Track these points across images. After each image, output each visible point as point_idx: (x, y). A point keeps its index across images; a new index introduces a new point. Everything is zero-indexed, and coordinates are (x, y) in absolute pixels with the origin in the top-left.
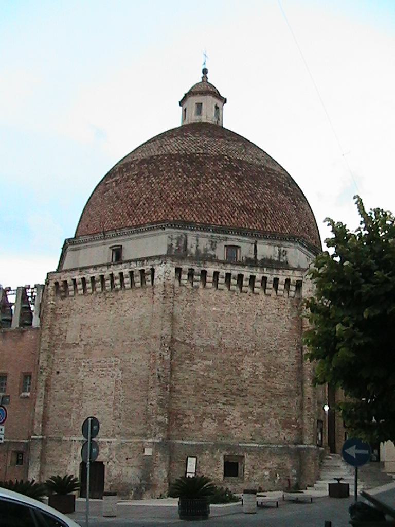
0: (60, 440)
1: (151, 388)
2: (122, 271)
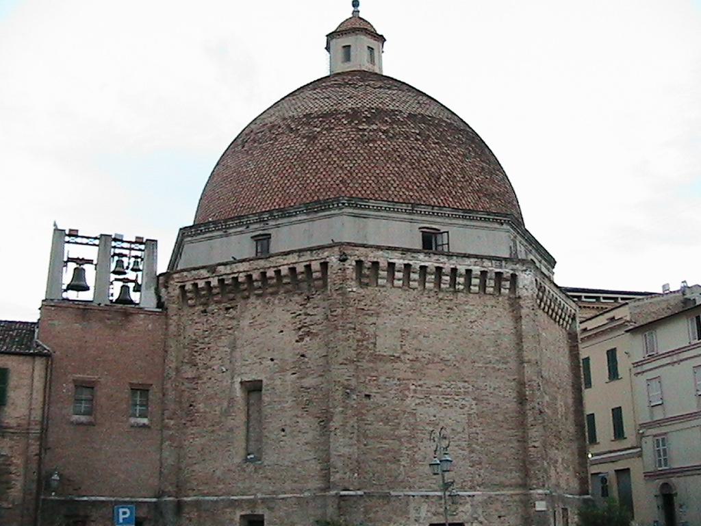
0: (387, 497)
1: (532, 425)
2: (470, 268)
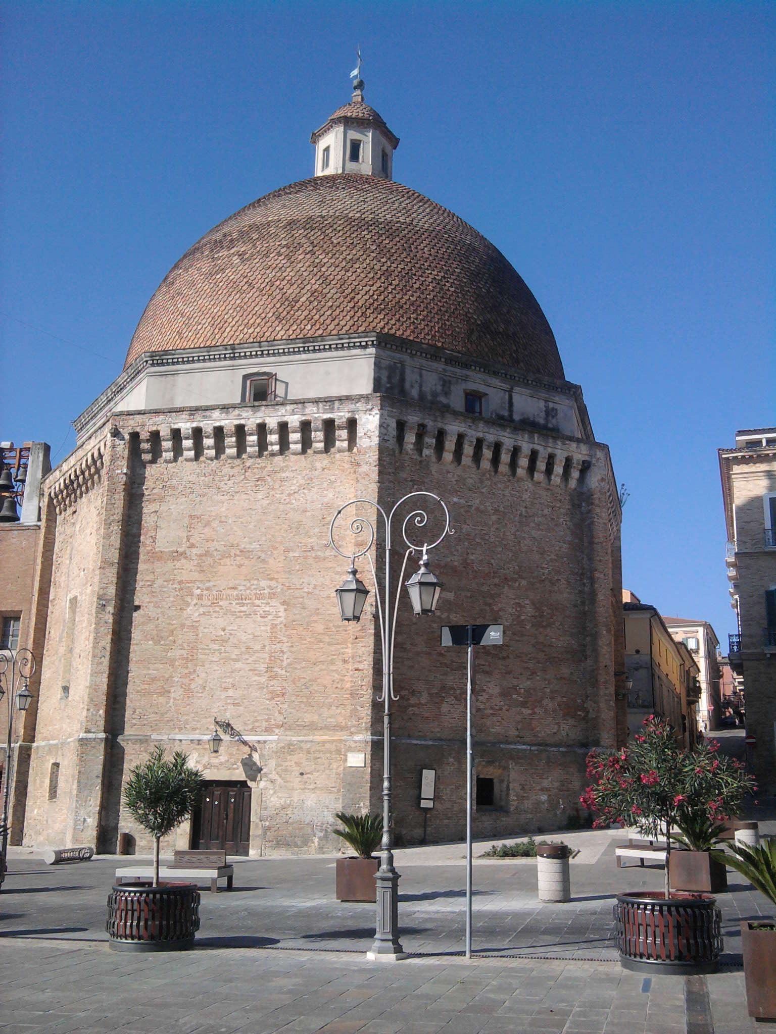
2: (285, 419)
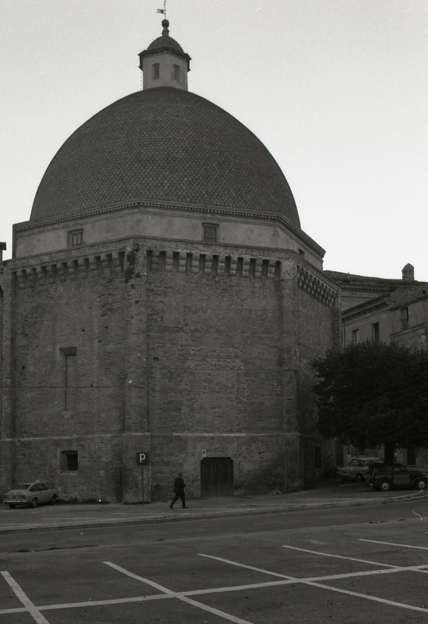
2: (242, 256)
